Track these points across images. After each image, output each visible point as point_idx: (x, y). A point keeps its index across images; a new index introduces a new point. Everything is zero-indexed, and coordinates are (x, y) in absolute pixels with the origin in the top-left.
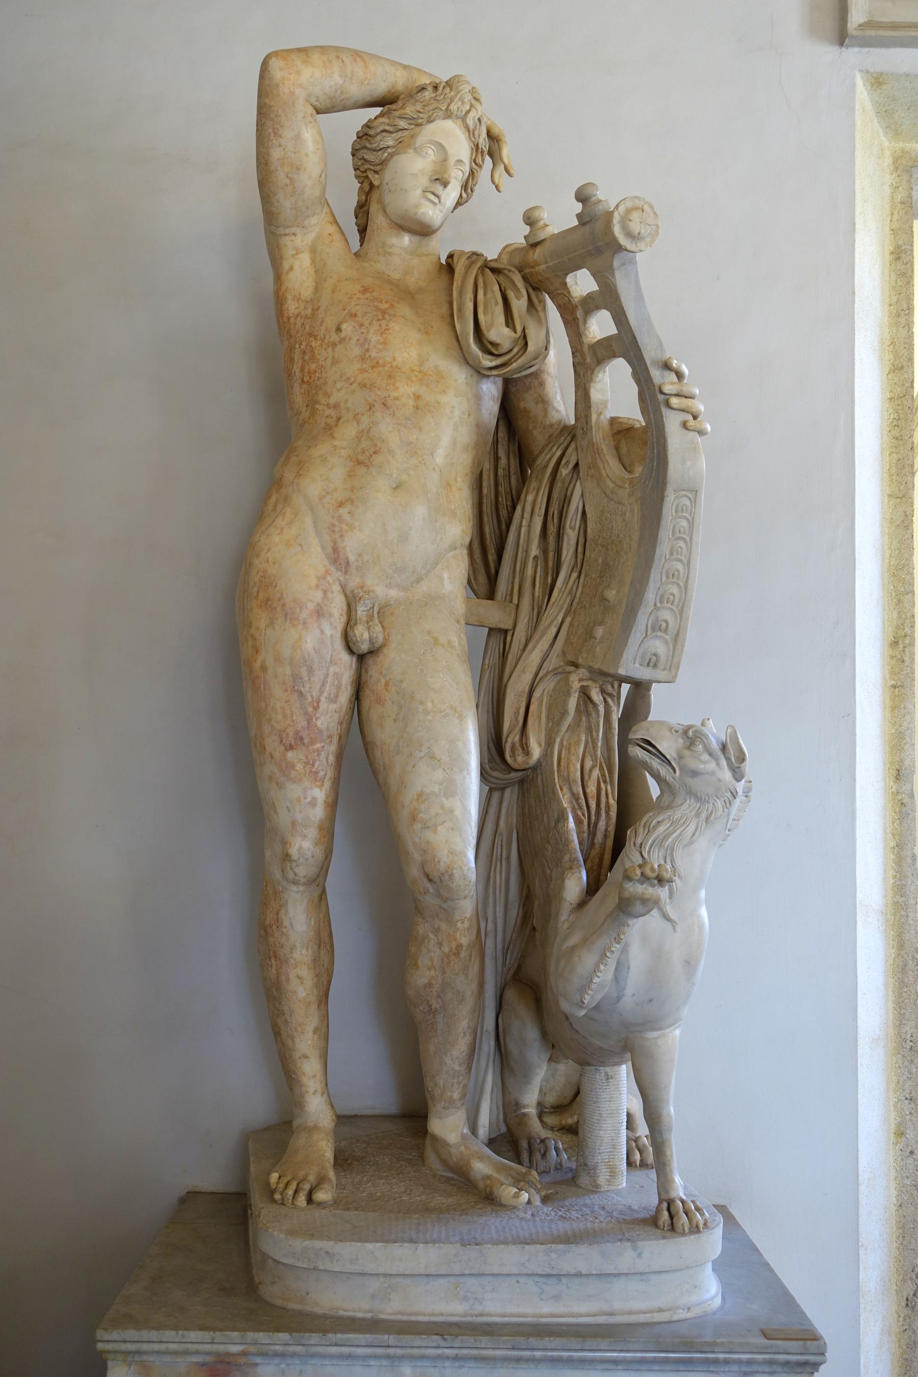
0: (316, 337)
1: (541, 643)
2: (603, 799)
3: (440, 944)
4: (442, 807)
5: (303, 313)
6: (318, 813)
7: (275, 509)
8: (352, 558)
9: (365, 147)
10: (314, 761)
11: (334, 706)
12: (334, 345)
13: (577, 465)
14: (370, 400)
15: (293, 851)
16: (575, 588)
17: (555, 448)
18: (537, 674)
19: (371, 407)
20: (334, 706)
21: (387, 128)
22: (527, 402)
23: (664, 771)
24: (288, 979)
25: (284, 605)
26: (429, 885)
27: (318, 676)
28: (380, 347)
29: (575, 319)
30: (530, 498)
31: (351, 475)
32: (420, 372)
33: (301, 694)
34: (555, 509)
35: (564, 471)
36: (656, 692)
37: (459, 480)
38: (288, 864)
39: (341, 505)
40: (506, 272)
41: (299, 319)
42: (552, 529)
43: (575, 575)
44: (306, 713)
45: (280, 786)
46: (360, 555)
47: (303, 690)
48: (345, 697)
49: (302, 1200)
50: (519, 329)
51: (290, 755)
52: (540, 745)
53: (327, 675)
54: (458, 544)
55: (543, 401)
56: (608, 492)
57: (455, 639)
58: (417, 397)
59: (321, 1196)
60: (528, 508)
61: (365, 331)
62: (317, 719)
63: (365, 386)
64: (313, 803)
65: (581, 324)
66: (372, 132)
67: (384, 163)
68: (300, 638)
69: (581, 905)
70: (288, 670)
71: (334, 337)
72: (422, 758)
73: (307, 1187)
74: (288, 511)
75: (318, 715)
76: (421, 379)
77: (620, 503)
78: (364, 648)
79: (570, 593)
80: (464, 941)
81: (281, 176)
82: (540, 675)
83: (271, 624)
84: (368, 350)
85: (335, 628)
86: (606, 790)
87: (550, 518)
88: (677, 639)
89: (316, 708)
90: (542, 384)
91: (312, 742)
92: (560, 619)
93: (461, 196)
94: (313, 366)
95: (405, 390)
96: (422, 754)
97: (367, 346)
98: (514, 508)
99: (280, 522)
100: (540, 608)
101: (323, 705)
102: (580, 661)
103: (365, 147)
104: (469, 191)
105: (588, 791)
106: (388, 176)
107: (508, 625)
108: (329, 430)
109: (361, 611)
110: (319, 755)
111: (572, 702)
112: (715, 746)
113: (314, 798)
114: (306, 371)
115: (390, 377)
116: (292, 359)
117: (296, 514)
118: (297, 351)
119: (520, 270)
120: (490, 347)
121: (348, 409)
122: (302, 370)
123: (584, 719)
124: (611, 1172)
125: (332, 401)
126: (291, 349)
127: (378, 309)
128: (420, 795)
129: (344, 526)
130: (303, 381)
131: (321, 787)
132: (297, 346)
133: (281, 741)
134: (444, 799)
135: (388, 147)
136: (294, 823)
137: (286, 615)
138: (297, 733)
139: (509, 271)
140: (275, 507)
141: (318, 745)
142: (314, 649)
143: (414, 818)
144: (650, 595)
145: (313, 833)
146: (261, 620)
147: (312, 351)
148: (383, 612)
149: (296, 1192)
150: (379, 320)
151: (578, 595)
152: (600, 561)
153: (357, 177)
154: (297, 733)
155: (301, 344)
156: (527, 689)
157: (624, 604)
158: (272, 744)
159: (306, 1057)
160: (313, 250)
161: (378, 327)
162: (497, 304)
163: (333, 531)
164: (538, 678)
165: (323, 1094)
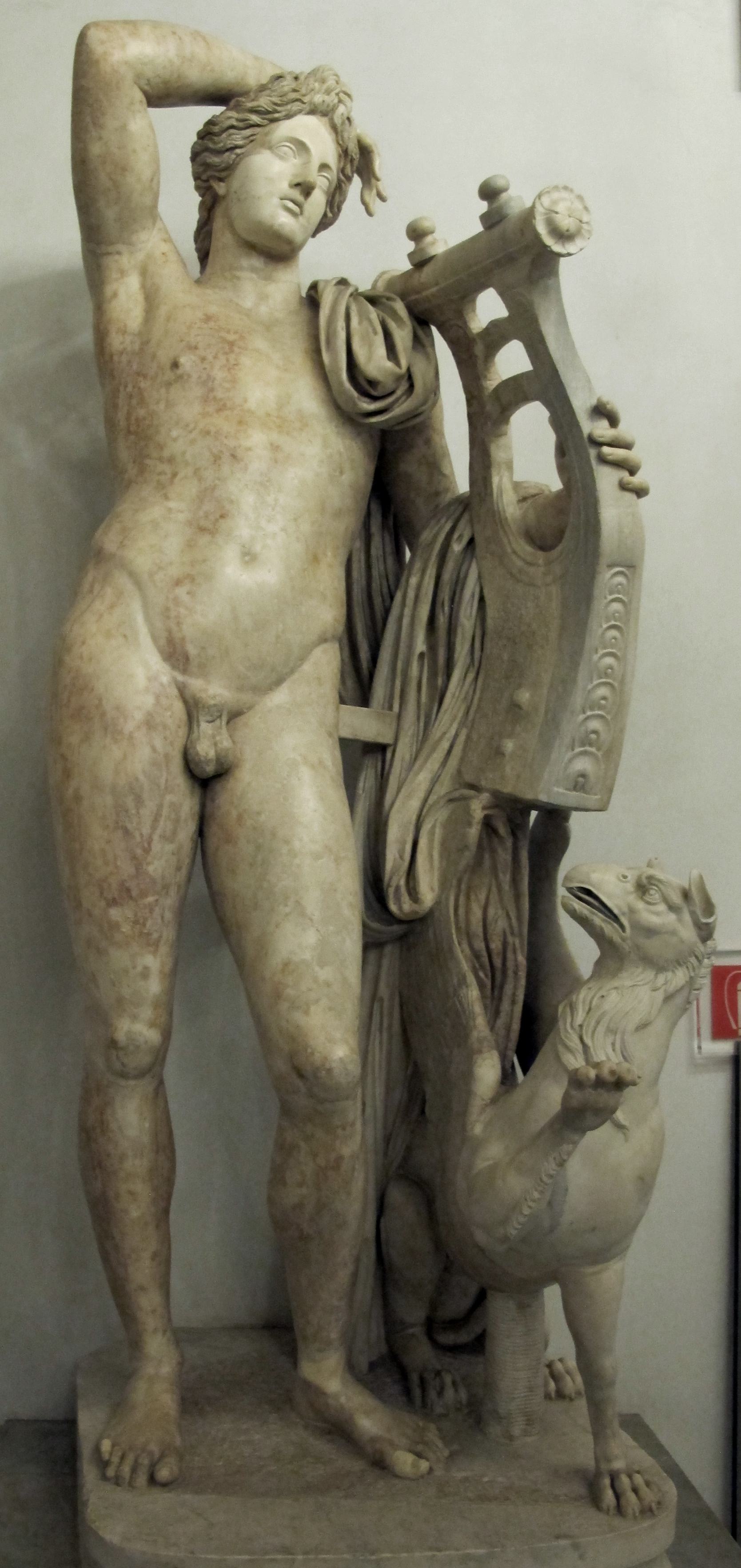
0: (145, 376)
1: (430, 761)
2: (510, 955)
3: (315, 1155)
4: (315, 980)
5: (129, 349)
6: (154, 987)
7: (91, 591)
8: (192, 650)
9: (207, 149)
10: (145, 919)
11: (170, 847)
12: (169, 384)
13: (471, 542)
14: (215, 451)
16: (471, 693)
17: (443, 521)
18: (425, 800)
19: (217, 459)
20: (170, 847)
21: (235, 123)
23: (609, 929)
24: (117, 1196)
25: (103, 714)
26: (299, 1083)
28: (227, 385)
29: (472, 357)
30: (414, 581)
31: (190, 545)
32: (278, 417)
33: (127, 832)
34: (445, 594)
35: (457, 547)
36: (576, 823)
37: (329, 554)
38: (114, 1052)
39: (178, 583)
40: (384, 300)
41: (124, 356)
42: (442, 620)
43: (471, 676)
44: (134, 858)
45: (101, 952)
46: (203, 648)
47: (129, 826)
49: (142, 1479)
50: (404, 363)
51: (115, 913)
52: (432, 889)
53: (160, 806)
54: (329, 635)
56: (515, 571)
58: (275, 448)
59: (164, 1474)
60: (411, 594)
61: (207, 366)
62: (148, 864)
63: (208, 433)
64: (145, 974)
65: (480, 362)
66: (216, 129)
67: (229, 169)
68: (125, 757)
69: (494, 1101)
70: (109, 800)
71: (169, 375)
72: (287, 915)
73: (145, 1461)
74: (109, 591)
75: (149, 859)
76: (280, 427)
77: (532, 584)
78: (210, 769)
79: (465, 698)
82: (430, 801)
83: (87, 738)
84: (212, 390)
85: (172, 744)
86: (514, 945)
87: (438, 605)
88: (610, 754)
89: (147, 851)
91: (143, 894)
92: (453, 731)
93: (325, 215)
94: (142, 412)
96: (287, 910)
97: (210, 383)
98: (392, 598)
99: (98, 606)
100: (428, 717)
101: (156, 846)
102: (483, 783)
103: (207, 149)
104: (336, 210)
105: (493, 946)
106: (236, 182)
110: (151, 911)
112: (676, 898)
113: (146, 968)
114: (133, 418)
115: (240, 423)
116: (115, 406)
117: (120, 594)
118: (122, 395)
119: (403, 297)
120: (367, 387)
121: (187, 464)
122: (128, 418)
123: (487, 856)
124: (528, 1420)
125: (166, 453)
126: (115, 393)
127: (224, 340)
128: (286, 964)
129: (182, 611)
130: (129, 432)
131: (155, 953)
132: (122, 389)
133: (102, 893)
134: (317, 969)
135: (236, 147)
136: (120, 1001)
137: (106, 729)
138: (122, 884)
139: (389, 299)
140: (92, 586)
141: (151, 899)
142: (144, 772)
143: (278, 995)
144: (578, 699)
145: (147, 1013)
147: (140, 391)
149: (134, 1470)
150: (226, 353)
151: (476, 701)
152: (506, 657)
153: (197, 188)
154: (122, 884)
155: (126, 386)
156: (414, 817)
157: (542, 710)
158: (89, 897)
159: (142, 1288)
160: (144, 273)
161: (225, 362)
162: (375, 333)
163: (168, 617)
164: (427, 806)
165: (165, 1332)
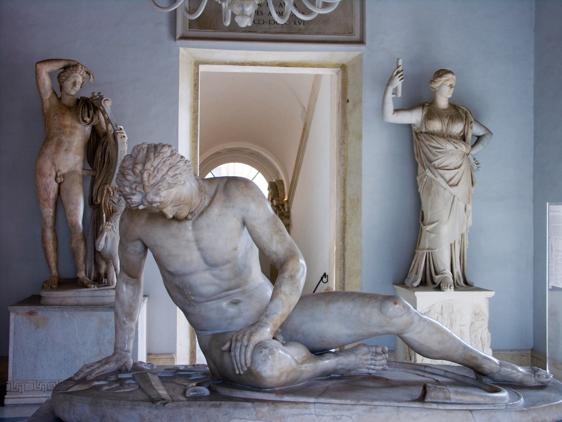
6: (52, 214)
15: (47, 222)
22: (98, 128)
27: (50, 188)
35: (105, 144)
48: (56, 191)
49: (49, 287)
55: (102, 128)
57: (78, 179)
58: (70, 131)
80: (80, 238)
81: (41, 86)
90: (101, 125)
95: (68, 130)
101: (51, 193)
107: (94, 174)
108: (52, 138)
109: (59, 174)
111: (105, 192)
146: (38, 176)
148: (64, 176)
158: (41, 201)
